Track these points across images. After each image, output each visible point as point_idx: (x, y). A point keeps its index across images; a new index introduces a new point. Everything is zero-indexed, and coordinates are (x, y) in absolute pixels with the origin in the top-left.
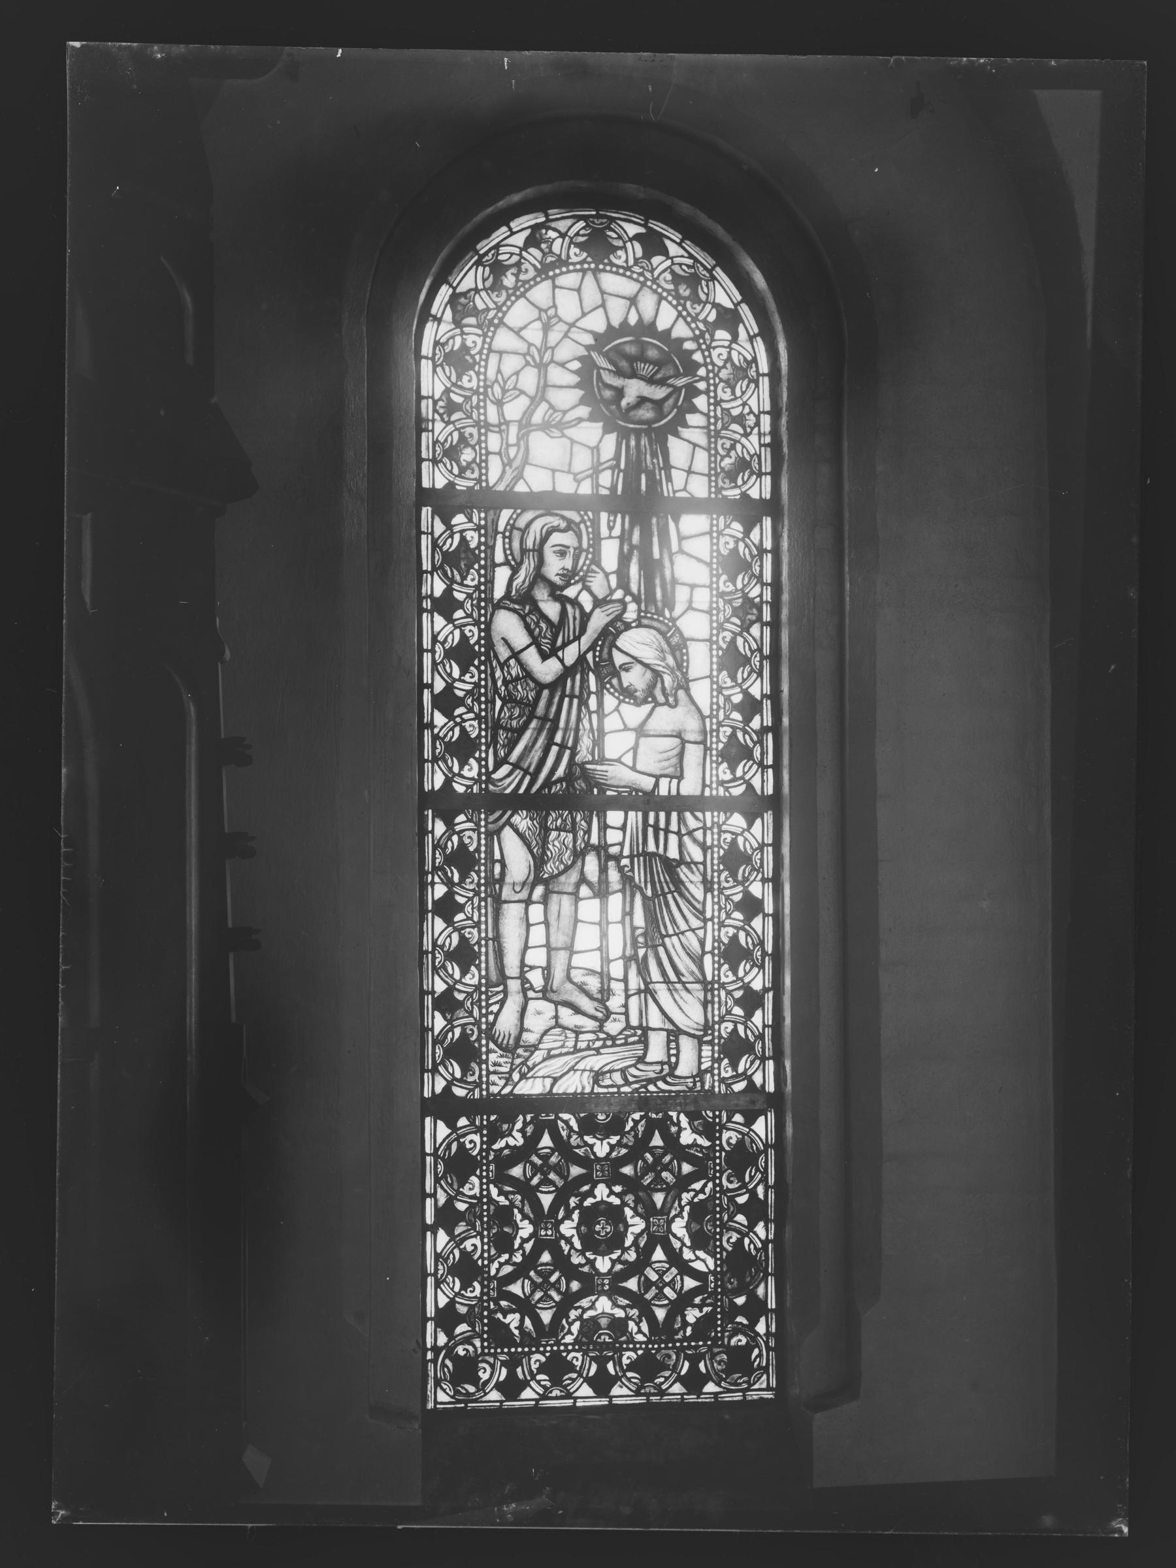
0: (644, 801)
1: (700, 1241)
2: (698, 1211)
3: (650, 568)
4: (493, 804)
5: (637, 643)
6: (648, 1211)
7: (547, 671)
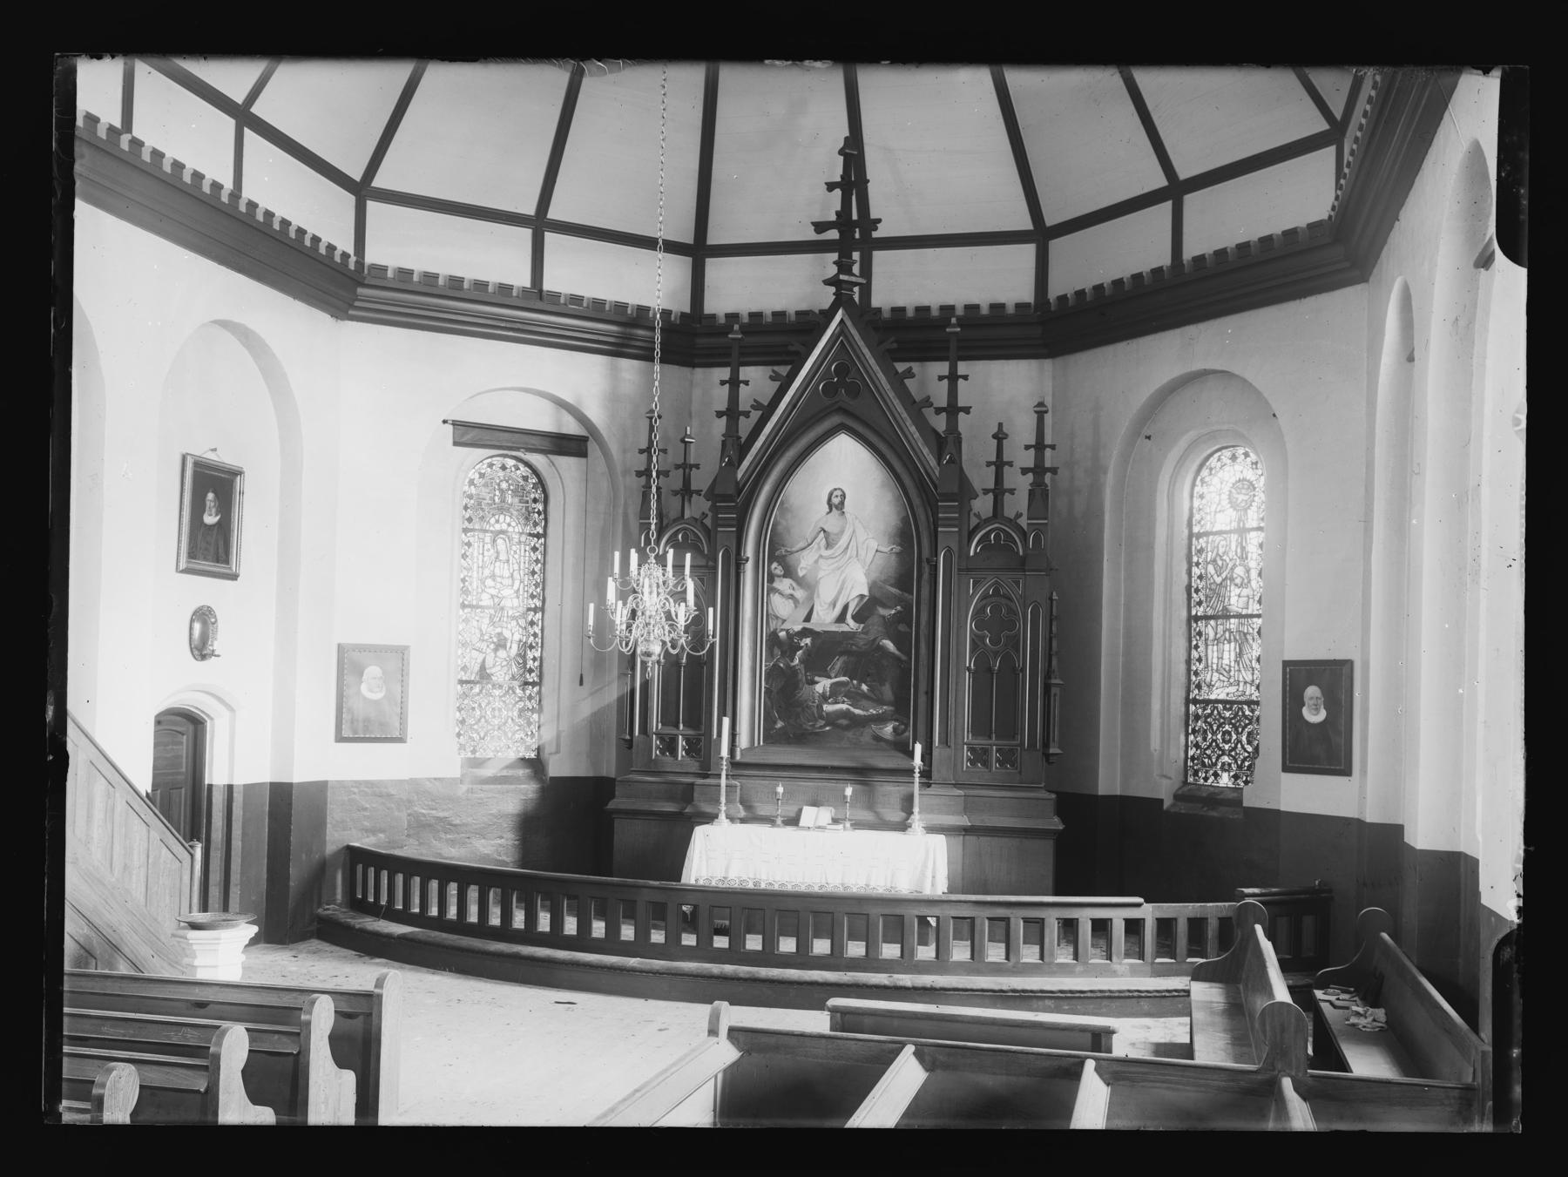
0: (1239, 616)
1: (1249, 743)
2: (1249, 734)
3: (1243, 548)
4: (1207, 618)
5: (1239, 571)
6: (1237, 733)
7: (1219, 580)
